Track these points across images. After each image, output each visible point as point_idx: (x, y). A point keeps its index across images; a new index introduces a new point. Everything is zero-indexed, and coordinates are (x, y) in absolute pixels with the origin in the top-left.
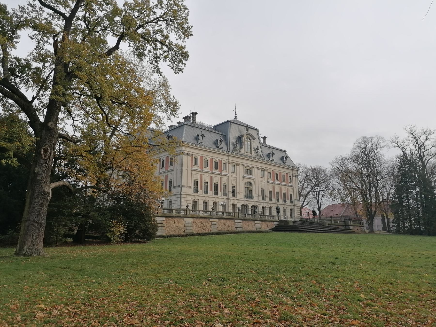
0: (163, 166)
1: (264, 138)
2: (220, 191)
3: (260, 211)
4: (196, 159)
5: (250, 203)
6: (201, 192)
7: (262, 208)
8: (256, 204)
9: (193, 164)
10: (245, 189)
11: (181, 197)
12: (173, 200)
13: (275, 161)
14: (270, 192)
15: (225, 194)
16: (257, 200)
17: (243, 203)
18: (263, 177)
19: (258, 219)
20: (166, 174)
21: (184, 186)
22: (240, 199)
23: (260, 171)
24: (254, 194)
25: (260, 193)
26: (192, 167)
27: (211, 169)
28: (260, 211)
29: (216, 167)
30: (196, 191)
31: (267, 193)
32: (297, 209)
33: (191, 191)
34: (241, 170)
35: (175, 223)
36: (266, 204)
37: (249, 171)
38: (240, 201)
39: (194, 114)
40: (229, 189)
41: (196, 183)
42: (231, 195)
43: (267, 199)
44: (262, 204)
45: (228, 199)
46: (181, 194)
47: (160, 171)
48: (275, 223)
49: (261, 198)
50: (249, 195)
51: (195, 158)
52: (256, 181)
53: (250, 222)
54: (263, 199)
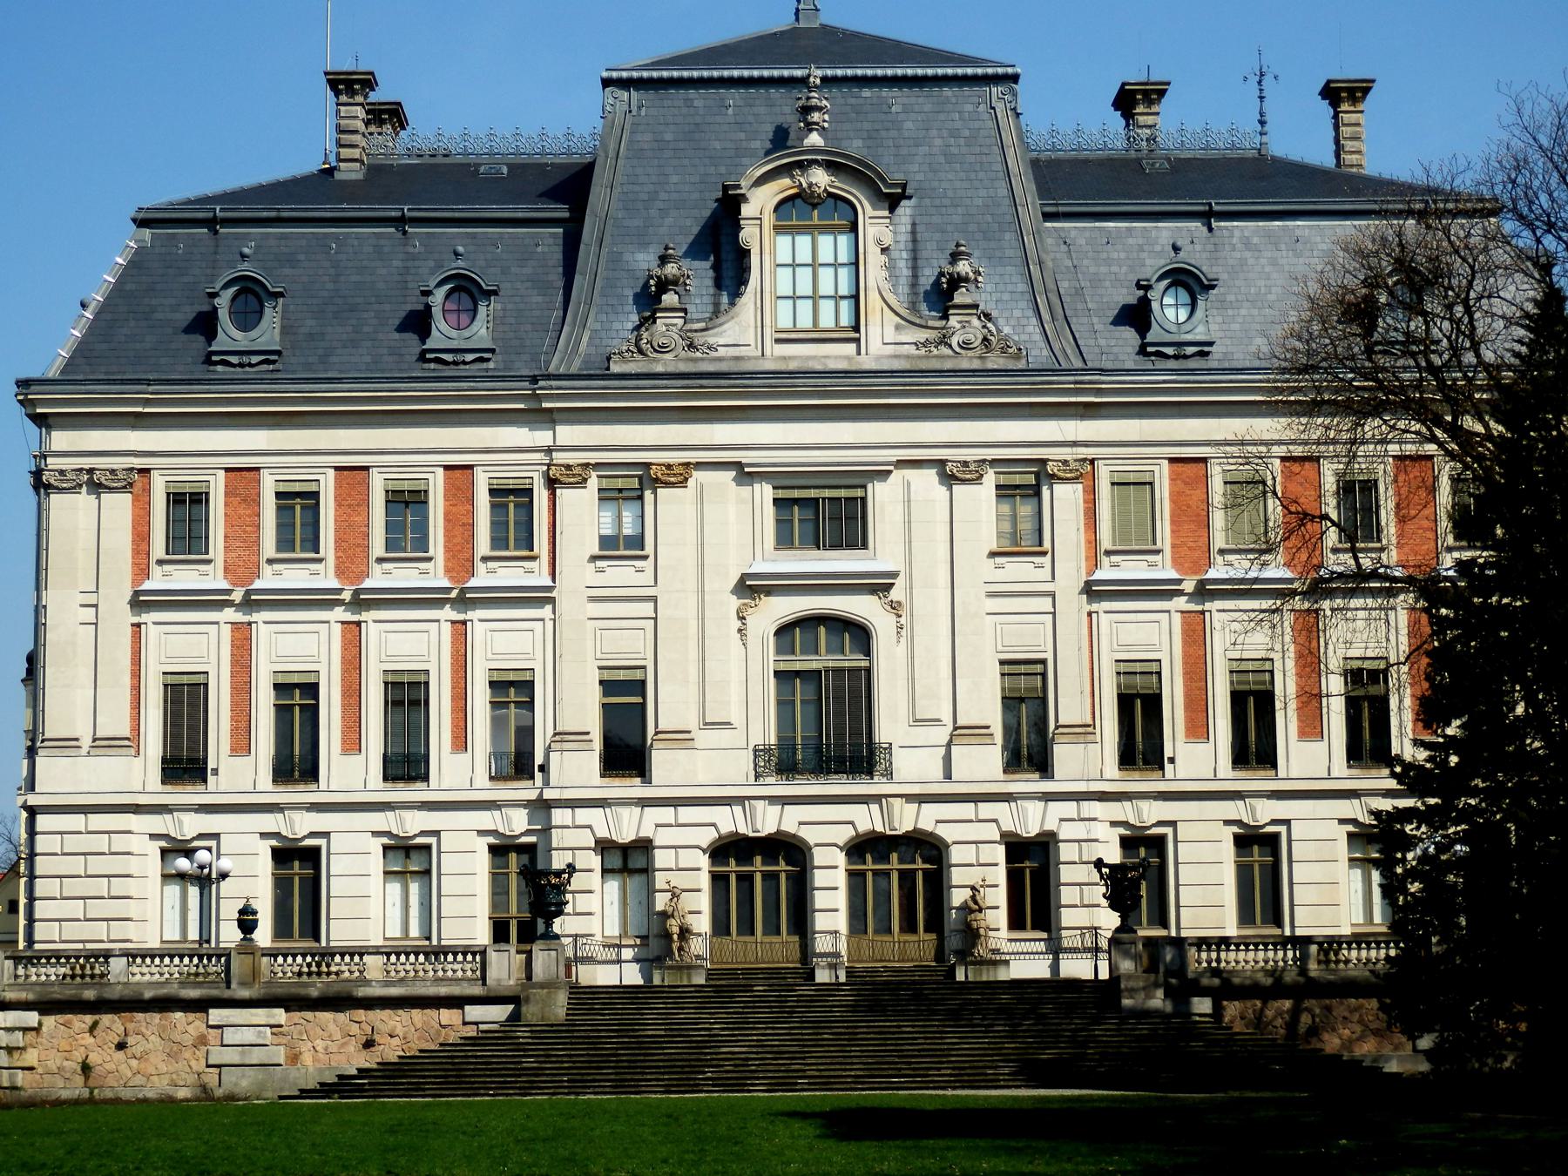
2: (461, 742)
5: (826, 823)
8: (927, 818)
9: (158, 548)
10: (766, 692)
11: (32, 832)
17: (729, 821)
18: (1026, 542)
19: (245, 993)
21: (68, 744)
23: (981, 499)
24: (889, 725)
26: (142, 571)
30: (185, 765)
31: (1082, 702)
33: (140, 773)
34: (720, 527)
37: (826, 511)
38: (688, 814)
41: (185, 700)
42: (576, 770)
48: (474, 1012)
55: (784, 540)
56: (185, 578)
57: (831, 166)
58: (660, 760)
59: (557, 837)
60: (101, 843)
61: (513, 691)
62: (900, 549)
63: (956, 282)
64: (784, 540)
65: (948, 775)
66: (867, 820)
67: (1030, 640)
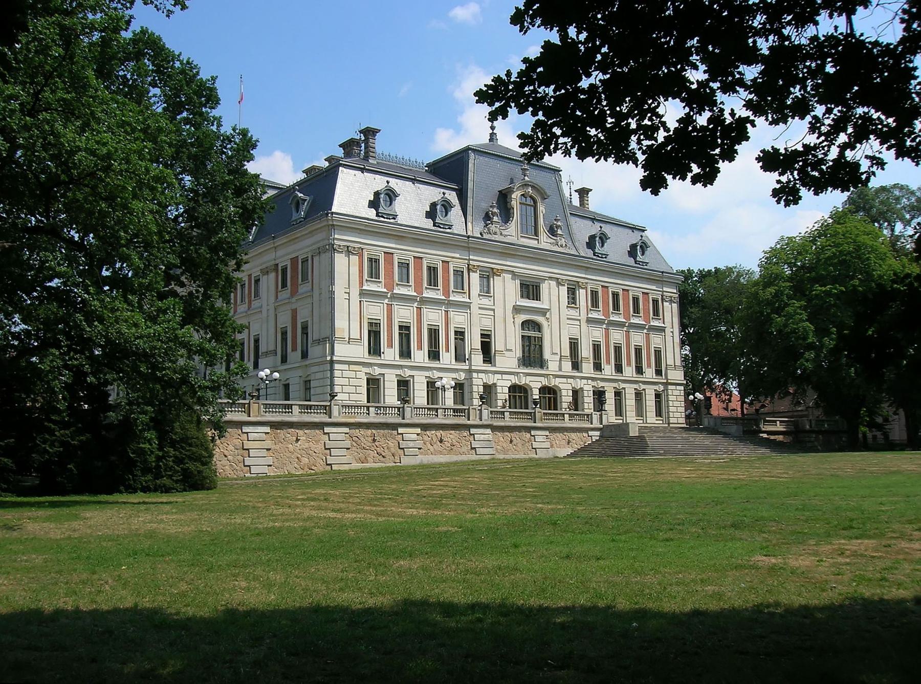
0: (284, 285)
1: (583, 193)
3: (566, 398)
4: (373, 262)
5: (535, 383)
6: (391, 354)
7: (571, 393)
9: (366, 277)
11: (332, 370)
12: (312, 378)
13: (609, 259)
14: (596, 348)
15: (460, 357)
16: (556, 370)
17: (514, 380)
20: (294, 307)
22: (507, 368)
23: (564, 290)
24: (547, 355)
25: (566, 352)
26: (361, 284)
27: (418, 288)
28: (566, 398)
29: (433, 282)
30: (375, 349)
31: (586, 352)
32: (676, 393)
33: (360, 351)
34: (507, 290)
35: (297, 440)
36: (584, 381)
37: (530, 289)
38: (505, 377)
39: (369, 133)
40: (474, 341)
42: (477, 360)
43: (588, 368)
44: (570, 380)
45: (470, 371)
46: (332, 362)
47: (277, 297)
49: (567, 366)
50: (532, 355)
51: (370, 260)
52: (555, 318)
53: (515, 435)
54: (576, 366)
55: (522, 297)
56: (373, 287)
57: (533, 187)
58: (498, 359)
59: (475, 381)
60: (353, 374)
61: (460, 334)
62: (548, 302)
63: (558, 227)
64: (522, 297)
65: (560, 370)
66: (545, 382)
67: (575, 332)
